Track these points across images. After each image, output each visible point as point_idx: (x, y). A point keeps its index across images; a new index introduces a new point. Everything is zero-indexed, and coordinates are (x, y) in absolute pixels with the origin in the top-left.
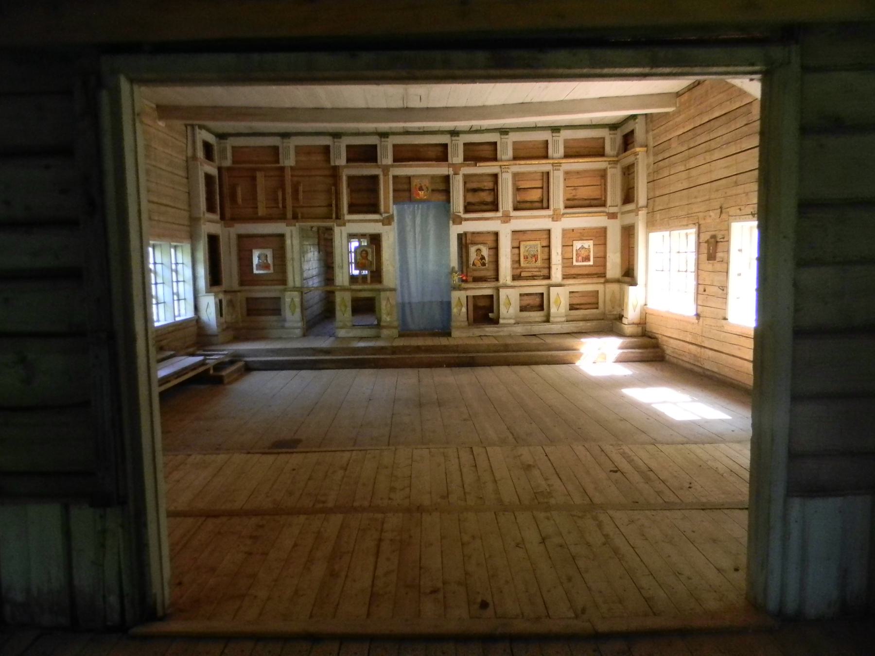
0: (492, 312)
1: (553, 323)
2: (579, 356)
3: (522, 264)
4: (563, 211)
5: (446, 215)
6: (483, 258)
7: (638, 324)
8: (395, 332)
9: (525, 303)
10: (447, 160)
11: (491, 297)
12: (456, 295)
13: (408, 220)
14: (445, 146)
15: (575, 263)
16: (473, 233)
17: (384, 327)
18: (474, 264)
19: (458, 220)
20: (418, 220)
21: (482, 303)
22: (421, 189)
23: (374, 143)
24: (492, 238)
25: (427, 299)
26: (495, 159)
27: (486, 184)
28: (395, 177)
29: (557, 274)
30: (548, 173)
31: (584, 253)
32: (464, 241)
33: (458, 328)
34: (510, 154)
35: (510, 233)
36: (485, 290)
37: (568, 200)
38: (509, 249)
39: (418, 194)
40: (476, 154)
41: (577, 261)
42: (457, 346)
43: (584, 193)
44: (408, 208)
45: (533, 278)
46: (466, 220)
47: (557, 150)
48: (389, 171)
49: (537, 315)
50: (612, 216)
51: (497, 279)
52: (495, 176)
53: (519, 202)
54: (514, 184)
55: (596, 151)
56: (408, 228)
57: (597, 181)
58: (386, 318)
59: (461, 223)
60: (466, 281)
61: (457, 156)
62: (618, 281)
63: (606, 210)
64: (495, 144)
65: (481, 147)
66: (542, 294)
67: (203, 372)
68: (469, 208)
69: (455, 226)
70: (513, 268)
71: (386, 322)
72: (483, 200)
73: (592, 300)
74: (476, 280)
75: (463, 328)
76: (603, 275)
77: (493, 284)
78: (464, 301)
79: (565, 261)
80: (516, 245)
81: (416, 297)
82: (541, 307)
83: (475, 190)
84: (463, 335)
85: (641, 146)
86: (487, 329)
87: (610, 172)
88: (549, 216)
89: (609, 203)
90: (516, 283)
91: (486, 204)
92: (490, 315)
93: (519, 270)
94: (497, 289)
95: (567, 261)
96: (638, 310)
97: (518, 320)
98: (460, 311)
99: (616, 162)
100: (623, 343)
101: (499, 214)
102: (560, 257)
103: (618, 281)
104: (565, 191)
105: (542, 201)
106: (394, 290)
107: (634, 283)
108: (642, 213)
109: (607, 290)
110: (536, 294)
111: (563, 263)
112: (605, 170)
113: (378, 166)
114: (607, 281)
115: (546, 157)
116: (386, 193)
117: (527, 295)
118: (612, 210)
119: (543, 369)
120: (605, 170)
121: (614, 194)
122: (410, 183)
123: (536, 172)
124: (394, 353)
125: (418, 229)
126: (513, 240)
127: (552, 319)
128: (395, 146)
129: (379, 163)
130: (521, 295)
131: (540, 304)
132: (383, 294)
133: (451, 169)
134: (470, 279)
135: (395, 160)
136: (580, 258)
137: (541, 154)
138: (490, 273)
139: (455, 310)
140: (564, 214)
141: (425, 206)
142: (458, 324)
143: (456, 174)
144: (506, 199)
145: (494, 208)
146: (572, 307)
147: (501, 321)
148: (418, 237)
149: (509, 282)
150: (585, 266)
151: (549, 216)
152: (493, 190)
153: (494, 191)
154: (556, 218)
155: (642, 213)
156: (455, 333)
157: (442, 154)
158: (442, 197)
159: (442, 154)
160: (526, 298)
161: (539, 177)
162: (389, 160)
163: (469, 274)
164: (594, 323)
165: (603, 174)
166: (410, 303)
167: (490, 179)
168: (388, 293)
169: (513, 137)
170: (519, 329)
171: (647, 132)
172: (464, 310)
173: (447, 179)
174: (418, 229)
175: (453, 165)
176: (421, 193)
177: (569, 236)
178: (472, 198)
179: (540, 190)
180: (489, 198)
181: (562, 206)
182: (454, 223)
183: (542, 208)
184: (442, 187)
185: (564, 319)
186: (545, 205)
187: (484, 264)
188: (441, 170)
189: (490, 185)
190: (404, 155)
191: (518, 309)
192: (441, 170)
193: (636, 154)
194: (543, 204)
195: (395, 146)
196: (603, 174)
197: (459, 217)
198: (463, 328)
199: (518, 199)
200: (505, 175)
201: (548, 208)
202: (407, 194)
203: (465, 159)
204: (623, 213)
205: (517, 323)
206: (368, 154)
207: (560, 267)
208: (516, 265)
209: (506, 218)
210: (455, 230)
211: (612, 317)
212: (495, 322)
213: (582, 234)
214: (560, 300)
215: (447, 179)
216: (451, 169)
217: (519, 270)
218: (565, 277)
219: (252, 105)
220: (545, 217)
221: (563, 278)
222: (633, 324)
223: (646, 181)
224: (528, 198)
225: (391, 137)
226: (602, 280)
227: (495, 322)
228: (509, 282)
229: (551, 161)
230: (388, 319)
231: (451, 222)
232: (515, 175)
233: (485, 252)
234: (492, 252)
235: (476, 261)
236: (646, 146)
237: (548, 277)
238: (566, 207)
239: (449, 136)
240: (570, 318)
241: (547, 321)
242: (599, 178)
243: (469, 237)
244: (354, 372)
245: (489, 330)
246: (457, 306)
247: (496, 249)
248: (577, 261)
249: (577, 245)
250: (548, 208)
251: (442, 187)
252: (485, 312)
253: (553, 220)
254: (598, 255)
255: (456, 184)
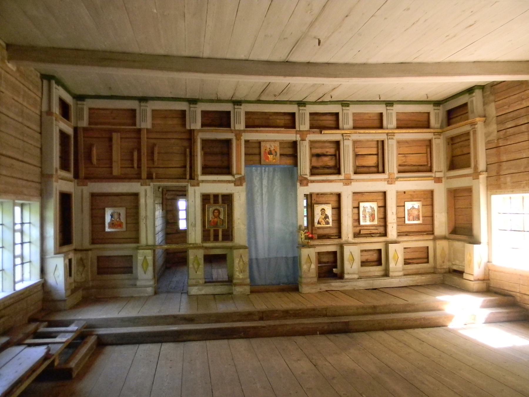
0: (336, 267)
1: (392, 277)
2: (450, 318)
3: (362, 223)
4: (396, 175)
5: (292, 176)
6: (326, 217)
7: (483, 280)
8: (247, 289)
9: (364, 258)
10: (294, 127)
11: (335, 253)
12: (305, 252)
13: (256, 181)
14: (293, 115)
15: (407, 222)
16: (318, 194)
17: (235, 285)
18: (319, 223)
19: (304, 182)
20: (265, 182)
21: (325, 259)
22: (270, 153)
23: (229, 110)
24: (335, 198)
25: (273, 255)
26: (337, 127)
27: (328, 150)
28: (247, 142)
29: (392, 232)
30: (383, 142)
31: (415, 213)
32: (312, 201)
33: (307, 284)
34: (351, 124)
35: (351, 194)
36: (329, 247)
37: (400, 165)
38: (350, 209)
39: (268, 158)
40: (319, 123)
41: (409, 220)
42: (326, 309)
43: (413, 159)
44: (256, 171)
45: (371, 235)
46: (313, 182)
47: (390, 122)
48: (241, 136)
49: (376, 270)
50: (438, 180)
51: (339, 236)
52: (337, 144)
53: (358, 167)
54: (354, 150)
55: (422, 123)
56: (256, 189)
57: (423, 150)
58: (239, 275)
59: (307, 185)
60: (312, 238)
61: (304, 124)
62: (445, 238)
63: (433, 175)
64: (337, 114)
65: (324, 118)
66: (380, 251)
67: (49, 366)
68: (314, 171)
69: (302, 188)
70: (355, 227)
71: (237, 279)
72: (329, 164)
73: (424, 256)
74: (322, 237)
75: (312, 284)
76: (431, 232)
77: (336, 241)
78: (314, 258)
79: (399, 220)
80: (356, 205)
81: (262, 254)
82: (379, 262)
83: (318, 156)
84: (313, 292)
85: (480, 116)
86: (333, 284)
87: (435, 143)
88: (385, 180)
89: (435, 168)
90: (357, 240)
91: (329, 168)
92: (334, 270)
93: (358, 228)
94: (341, 246)
95: (401, 219)
96: (482, 266)
97: (362, 275)
98: (309, 266)
99: (440, 134)
100: (485, 300)
101: (342, 177)
102: (395, 217)
103: (445, 238)
104: (398, 158)
105: (377, 166)
106: (245, 247)
107: (475, 241)
108: (483, 177)
109: (438, 246)
110: (374, 250)
111: (397, 222)
112: (430, 141)
113: (232, 132)
114: (435, 239)
115: (381, 127)
116: (238, 158)
117: (366, 251)
118: (438, 175)
119: (421, 333)
120: (430, 141)
121: (440, 160)
122: (260, 147)
123: (372, 141)
124: (261, 319)
125: (265, 190)
126: (354, 200)
127: (391, 274)
128: (247, 113)
129: (232, 128)
130: (362, 251)
131: (379, 259)
132: (236, 253)
133: (298, 136)
134: (316, 236)
135: (247, 127)
136: (411, 218)
137: (374, 125)
138: (334, 231)
139: (305, 267)
140: (398, 178)
141: (271, 169)
142: (309, 280)
143: (303, 140)
144: (348, 163)
145: (335, 171)
146: (407, 262)
147: (346, 276)
148: (265, 197)
149: (351, 239)
150: (415, 224)
151: (385, 180)
152: (335, 155)
153: (337, 156)
154: (391, 181)
155: (483, 177)
156: (305, 289)
157: (291, 121)
158: (289, 161)
159: (291, 121)
160: (365, 253)
161: (374, 144)
162: (241, 126)
163: (314, 232)
164: (429, 276)
165: (429, 144)
166: (257, 259)
167: (332, 145)
168: (241, 251)
169: (353, 109)
170: (362, 284)
171: (485, 104)
172: (313, 266)
173: (294, 145)
174: (265, 190)
175: (300, 132)
176: (270, 157)
177: (403, 197)
178: (317, 163)
179: (375, 157)
180: (331, 163)
181: (396, 171)
182: (301, 184)
183: (378, 172)
184: (289, 151)
185: (401, 273)
186: (381, 169)
187: (328, 223)
188: (289, 136)
189: (331, 151)
190: (255, 122)
191: (360, 263)
192: (289, 136)
193: (473, 124)
194: (379, 168)
195: (247, 113)
196: (429, 144)
197: (306, 179)
198: (312, 284)
199: (357, 164)
200: (346, 143)
201: (383, 172)
202: (257, 158)
203: (311, 128)
204: (448, 178)
205: (360, 278)
206: (223, 120)
207: (395, 226)
208: (357, 224)
209: (348, 181)
210: (302, 191)
211: (443, 271)
212: (340, 276)
213: (413, 196)
214: (396, 255)
215: (294, 145)
216: (298, 136)
217: (358, 228)
218: (400, 234)
219: (119, 49)
220: (381, 180)
221: (398, 236)
222: (479, 280)
223: (484, 148)
224: (365, 164)
225: (243, 105)
226: (431, 237)
227: (340, 276)
228: (351, 239)
229: (387, 131)
230: (241, 276)
231: (298, 184)
232: (355, 142)
233: (329, 211)
234: (335, 211)
235: (320, 220)
236: (485, 116)
237: (385, 234)
238: (399, 172)
239: (296, 106)
240: (406, 273)
241: (386, 274)
242: (425, 148)
243: (314, 197)
244: (224, 343)
245: (336, 285)
246: (306, 263)
247: (338, 209)
248: (409, 220)
249: (409, 205)
250: (383, 172)
251: (289, 151)
252: (331, 268)
253: (388, 184)
254: (426, 215)
255: (303, 148)
